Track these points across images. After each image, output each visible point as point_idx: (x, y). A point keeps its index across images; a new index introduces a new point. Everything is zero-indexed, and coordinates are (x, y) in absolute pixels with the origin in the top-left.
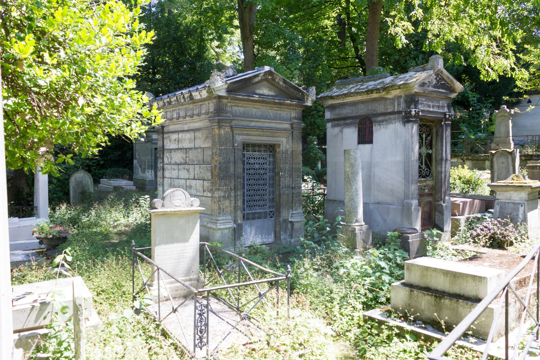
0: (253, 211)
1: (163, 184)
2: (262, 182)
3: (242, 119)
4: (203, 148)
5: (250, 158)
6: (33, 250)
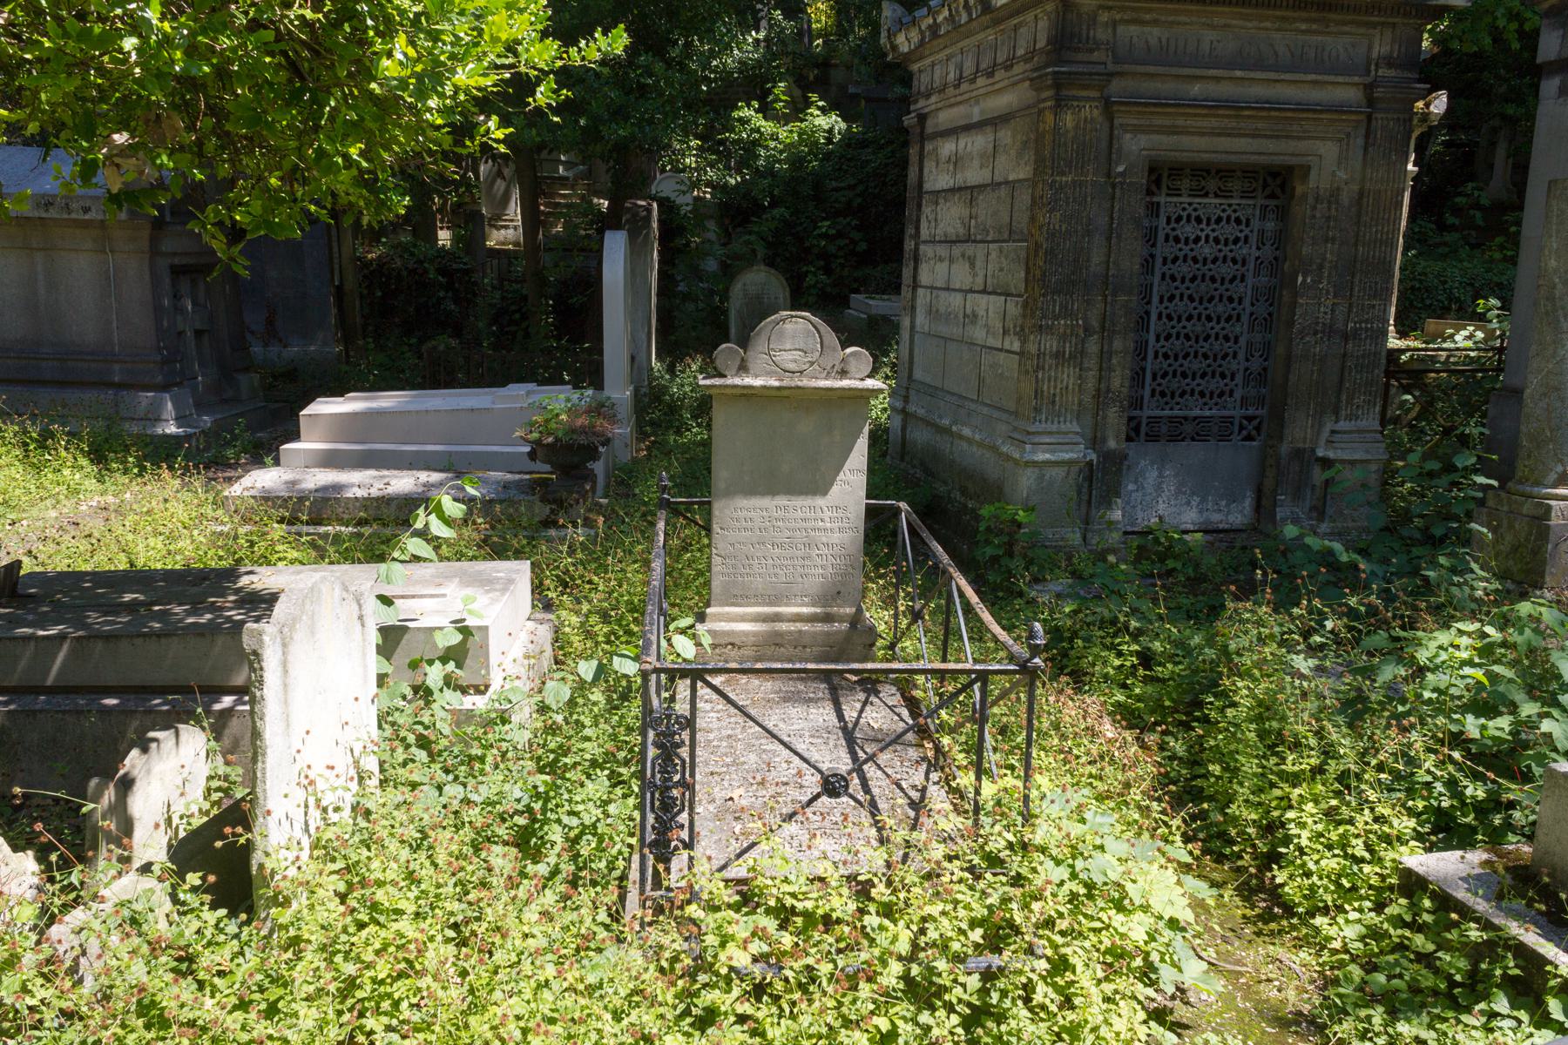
0: (1176, 412)
1: (913, 308)
2: (1220, 308)
3: (1151, 69)
4: (1015, 182)
5: (1179, 219)
6: (531, 473)
